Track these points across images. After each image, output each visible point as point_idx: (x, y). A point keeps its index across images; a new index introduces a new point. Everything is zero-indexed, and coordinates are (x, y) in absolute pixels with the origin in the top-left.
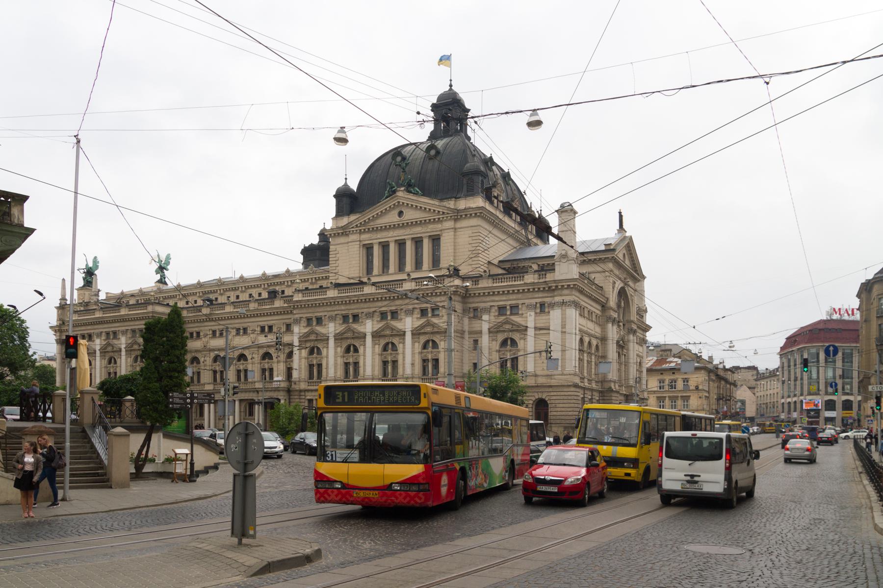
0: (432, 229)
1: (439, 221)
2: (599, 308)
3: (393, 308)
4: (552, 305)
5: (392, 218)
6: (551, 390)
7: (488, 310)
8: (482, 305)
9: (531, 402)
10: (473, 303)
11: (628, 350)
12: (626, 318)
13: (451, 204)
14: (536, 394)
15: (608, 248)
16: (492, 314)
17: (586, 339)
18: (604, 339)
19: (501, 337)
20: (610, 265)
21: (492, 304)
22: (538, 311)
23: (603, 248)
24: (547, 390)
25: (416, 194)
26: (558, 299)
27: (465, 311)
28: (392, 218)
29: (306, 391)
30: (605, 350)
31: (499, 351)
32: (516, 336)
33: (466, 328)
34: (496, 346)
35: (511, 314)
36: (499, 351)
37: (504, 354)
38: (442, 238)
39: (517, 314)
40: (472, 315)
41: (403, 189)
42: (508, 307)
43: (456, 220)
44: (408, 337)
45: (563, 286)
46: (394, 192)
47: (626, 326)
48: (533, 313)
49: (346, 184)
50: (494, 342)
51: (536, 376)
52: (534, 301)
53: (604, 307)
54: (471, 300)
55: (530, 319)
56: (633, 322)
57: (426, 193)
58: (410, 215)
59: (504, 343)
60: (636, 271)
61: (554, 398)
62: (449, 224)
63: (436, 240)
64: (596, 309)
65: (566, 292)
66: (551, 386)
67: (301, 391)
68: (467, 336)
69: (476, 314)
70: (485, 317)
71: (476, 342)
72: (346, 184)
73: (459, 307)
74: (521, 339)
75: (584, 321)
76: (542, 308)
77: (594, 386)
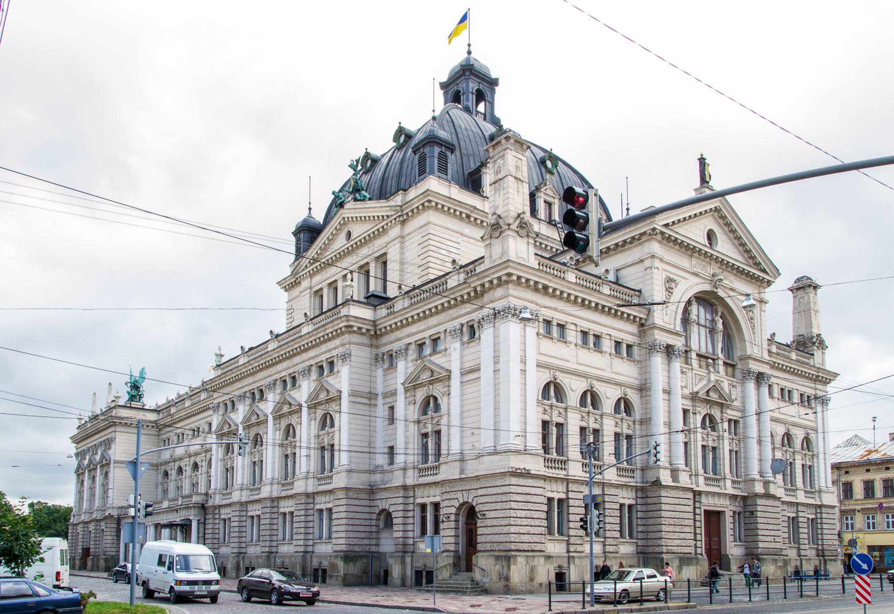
1: (384, 231)
2: (633, 328)
8: (395, 346)
9: (453, 510)
10: (386, 344)
11: (743, 410)
12: (738, 353)
14: (459, 495)
16: (410, 358)
17: (574, 388)
18: (644, 389)
21: (408, 340)
22: (466, 338)
24: (475, 485)
27: (377, 359)
28: (341, 242)
30: (647, 406)
31: (419, 422)
32: (437, 390)
33: (380, 389)
34: (414, 413)
36: (419, 422)
38: (389, 257)
40: (386, 365)
42: (427, 342)
43: (403, 222)
48: (457, 345)
50: (412, 407)
52: (456, 323)
54: (385, 339)
56: (749, 357)
58: (358, 230)
61: (484, 499)
64: (626, 332)
66: (477, 478)
68: (380, 401)
73: (361, 354)
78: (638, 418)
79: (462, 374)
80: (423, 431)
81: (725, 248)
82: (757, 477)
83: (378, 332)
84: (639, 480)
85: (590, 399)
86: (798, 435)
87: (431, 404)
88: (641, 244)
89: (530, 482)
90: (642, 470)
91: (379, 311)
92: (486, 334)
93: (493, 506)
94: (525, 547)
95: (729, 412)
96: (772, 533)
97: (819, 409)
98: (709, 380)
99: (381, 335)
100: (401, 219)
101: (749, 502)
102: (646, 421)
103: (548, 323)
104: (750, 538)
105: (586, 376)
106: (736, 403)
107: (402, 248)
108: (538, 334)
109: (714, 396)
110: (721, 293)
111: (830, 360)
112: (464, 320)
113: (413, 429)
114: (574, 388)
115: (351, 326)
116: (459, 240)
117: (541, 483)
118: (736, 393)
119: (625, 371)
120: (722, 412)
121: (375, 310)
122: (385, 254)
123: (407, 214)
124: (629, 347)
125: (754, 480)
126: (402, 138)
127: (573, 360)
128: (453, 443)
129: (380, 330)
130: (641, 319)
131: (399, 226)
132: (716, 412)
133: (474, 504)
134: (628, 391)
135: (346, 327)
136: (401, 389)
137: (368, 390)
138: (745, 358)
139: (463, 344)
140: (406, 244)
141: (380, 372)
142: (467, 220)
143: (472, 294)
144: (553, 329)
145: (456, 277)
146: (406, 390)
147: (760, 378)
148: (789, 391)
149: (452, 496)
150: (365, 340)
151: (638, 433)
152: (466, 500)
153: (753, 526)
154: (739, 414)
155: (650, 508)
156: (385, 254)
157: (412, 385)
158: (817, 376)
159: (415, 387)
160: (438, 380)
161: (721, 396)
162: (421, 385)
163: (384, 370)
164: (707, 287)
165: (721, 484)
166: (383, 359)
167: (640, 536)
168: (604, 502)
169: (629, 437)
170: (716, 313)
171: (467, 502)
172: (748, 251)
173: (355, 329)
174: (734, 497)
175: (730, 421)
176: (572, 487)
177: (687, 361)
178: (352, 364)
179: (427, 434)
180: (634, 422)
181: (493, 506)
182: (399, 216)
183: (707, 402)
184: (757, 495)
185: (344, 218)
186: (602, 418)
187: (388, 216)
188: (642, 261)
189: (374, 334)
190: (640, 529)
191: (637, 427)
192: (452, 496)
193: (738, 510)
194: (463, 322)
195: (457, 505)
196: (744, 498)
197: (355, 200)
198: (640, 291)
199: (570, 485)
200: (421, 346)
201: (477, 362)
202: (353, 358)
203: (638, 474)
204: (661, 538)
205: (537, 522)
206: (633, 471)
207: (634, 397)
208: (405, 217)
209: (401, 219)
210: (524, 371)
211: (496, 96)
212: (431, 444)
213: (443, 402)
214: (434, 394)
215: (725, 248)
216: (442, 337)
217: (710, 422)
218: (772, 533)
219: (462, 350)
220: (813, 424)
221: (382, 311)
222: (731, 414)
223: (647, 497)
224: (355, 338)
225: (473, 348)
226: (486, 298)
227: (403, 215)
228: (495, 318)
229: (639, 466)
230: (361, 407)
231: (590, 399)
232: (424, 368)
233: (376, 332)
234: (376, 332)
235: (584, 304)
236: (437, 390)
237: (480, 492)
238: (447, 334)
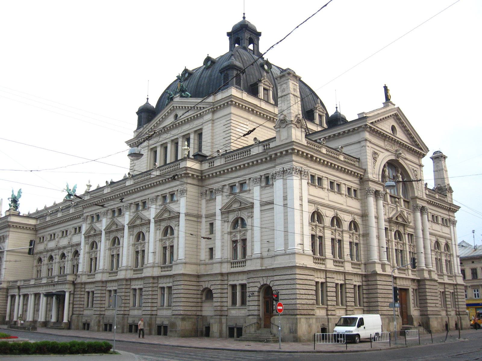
0: (196, 125)
1: (201, 116)
2: (357, 180)
3: (143, 198)
4: (274, 177)
5: (170, 120)
6: (275, 273)
7: (221, 190)
8: (215, 186)
9: (257, 289)
10: (209, 185)
13: (211, 99)
14: (261, 279)
15: (361, 116)
17: (328, 214)
18: (364, 216)
19: (232, 217)
20: (367, 135)
21: (223, 183)
22: (263, 184)
23: (357, 117)
24: (271, 274)
25: (187, 97)
26: (279, 168)
29: (85, 283)
30: (367, 226)
32: (244, 215)
33: (204, 213)
34: (228, 227)
35: (242, 191)
36: (230, 233)
37: (235, 236)
38: (203, 131)
39: (246, 191)
41: (178, 95)
43: (214, 112)
44: (152, 225)
45: (281, 153)
46: (172, 99)
47: (411, 203)
49: (147, 103)
51: (262, 258)
52: (257, 175)
53: (363, 180)
55: (256, 194)
56: (417, 198)
57: (195, 95)
59: (235, 223)
60: (417, 146)
62: (209, 117)
63: (199, 134)
65: (286, 159)
66: (273, 269)
67: (82, 284)
68: (204, 220)
69: (210, 194)
70: (219, 198)
71: (212, 225)
72: (147, 103)
73: (192, 190)
74: (248, 217)
75: (316, 191)
76: (268, 181)
77: (348, 268)
78: (361, 232)
79: (261, 205)
80: (234, 239)
81: (400, 135)
82: (425, 268)
83: (203, 178)
84: (363, 270)
85: (337, 221)
86: (443, 242)
87: (239, 223)
88: (359, 132)
89: (307, 272)
90: (365, 264)
91: (204, 165)
92: (278, 184)
93: (285, 287)
94: (305, 312)
95: (408, 229)
96: (435, 301)
97: (452, 227)
98: (397, 210)
99: (205, 179)
100: (213, 110)
101: (421, 283)
102: (366, 235)
103: (313, 177)
104: (422, 305)
105: (333, 208)
106: (411, 224)
107: (212, 126)
108: (308, 183)
109: (400, 220)
110: (401, 161)
111: (456, 198)
112: (262, 173)
113: (227, 238)
114: (328, 214)
115: (189, 173)
116: (248, 124)
117: (312, 273)
118: (411, 218)
119: (354, 205)
120: (404, 230)
121: (201, 164)
122: (201, 129)
123: (217, 107)
124: (355, 191)
125: (423, 270)
126: (209, 63)
127: (326, 198)
128: (256, 248)
129: (205, 176)
130: (361, 175)
131: (211, 114)
132: (401, 229)
133: (271, 285)
134: (356, 217)
135: (185, 174)
136: (218, 213)
137: (196, 212)
138: (415, 198)
139: (261, 187)
140: (215, 124)
141: (204, 201)
142: (251, 112)
143: (268, 159)
144: (316, 181)
145: (257, 148)
146: (222, 213)
147: (423, 210)
148: (436, 217)
149: (256, 280)
150: (195, 182)
151: (361, 242)
152: (265, 283)
153: (424, 298)
154: (412, 230)
155: (370, 287)
156: (201, 129)
157: (226, 211)
158: (450, 208)
159: (228, 212)
160: (245, 208)
161: (404, 220)
162: (233, 211)
163: (207, 201)
164: (393, 157)
165: (406, 272)
166: (206, 193)
167: (365, 304)
168: (346, 284)
169: (357, 244)
170: (398, 172)
171: (266, 284)
172: (413, 138)
173: (190, 175)
174: (413, 280)
175: (408, 234)
176: (329, 275)
177: (385, 200)
178: (188, 196)
179: (237, 241)
180: (359, 235)
181: (285, 287)
182: (212, 108)
183: (397, 223)
184: (425, 279)
185: (173, 107)
186: (342, 233)
187: (204, 108)
188: (359, 142)
189: (201, 178)
190: (365, 300)
191: (361, 238)
192: (256, 280)
193: (415, 288)
194: (262, 174)
195: (259, 285)
196: (418, 281)
197: (181, 96)
198: (359, 159)
199: (327, 274)
200: (232, 187)
201: (271, 198)
202: (188, 193)
203: (362, 266)
204: (378, 306)
205: (311, 297)
206: (359, 265)
207: (358, 220)
208: (215, 109)
209: (213, 110)
210: (301, 205)
211: (260, 42)
212: (239, 246)
213: (248, 222)
214: (242, 216)
215: (400, 135)
216: (247, 182)
217: (399, 235)
218: (435, 301)
219: (261, 191)
220: (449, 236)
221: (206, 166)
222: (410, 230)
223: (368, 281)
224: (190, 181)
225: (268, 190)
226: (278, 161)
227: (214, 108)
228: (283, 174)
229: (363, 262)
230: (193, 223)
231: (337, 221)
232: (235, 201)
233: (202, 177)
234: (202, 177)
235: (332, 166)
236: (244, 215)
237: (276, 278)
238: (251, 181)
